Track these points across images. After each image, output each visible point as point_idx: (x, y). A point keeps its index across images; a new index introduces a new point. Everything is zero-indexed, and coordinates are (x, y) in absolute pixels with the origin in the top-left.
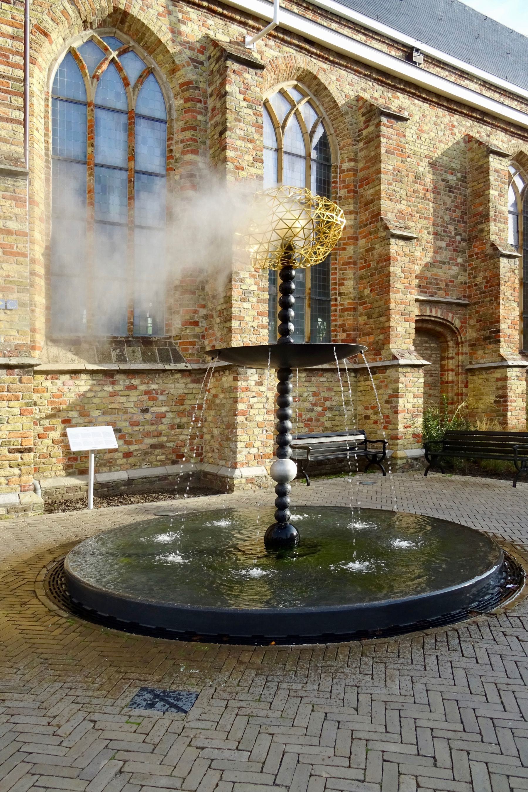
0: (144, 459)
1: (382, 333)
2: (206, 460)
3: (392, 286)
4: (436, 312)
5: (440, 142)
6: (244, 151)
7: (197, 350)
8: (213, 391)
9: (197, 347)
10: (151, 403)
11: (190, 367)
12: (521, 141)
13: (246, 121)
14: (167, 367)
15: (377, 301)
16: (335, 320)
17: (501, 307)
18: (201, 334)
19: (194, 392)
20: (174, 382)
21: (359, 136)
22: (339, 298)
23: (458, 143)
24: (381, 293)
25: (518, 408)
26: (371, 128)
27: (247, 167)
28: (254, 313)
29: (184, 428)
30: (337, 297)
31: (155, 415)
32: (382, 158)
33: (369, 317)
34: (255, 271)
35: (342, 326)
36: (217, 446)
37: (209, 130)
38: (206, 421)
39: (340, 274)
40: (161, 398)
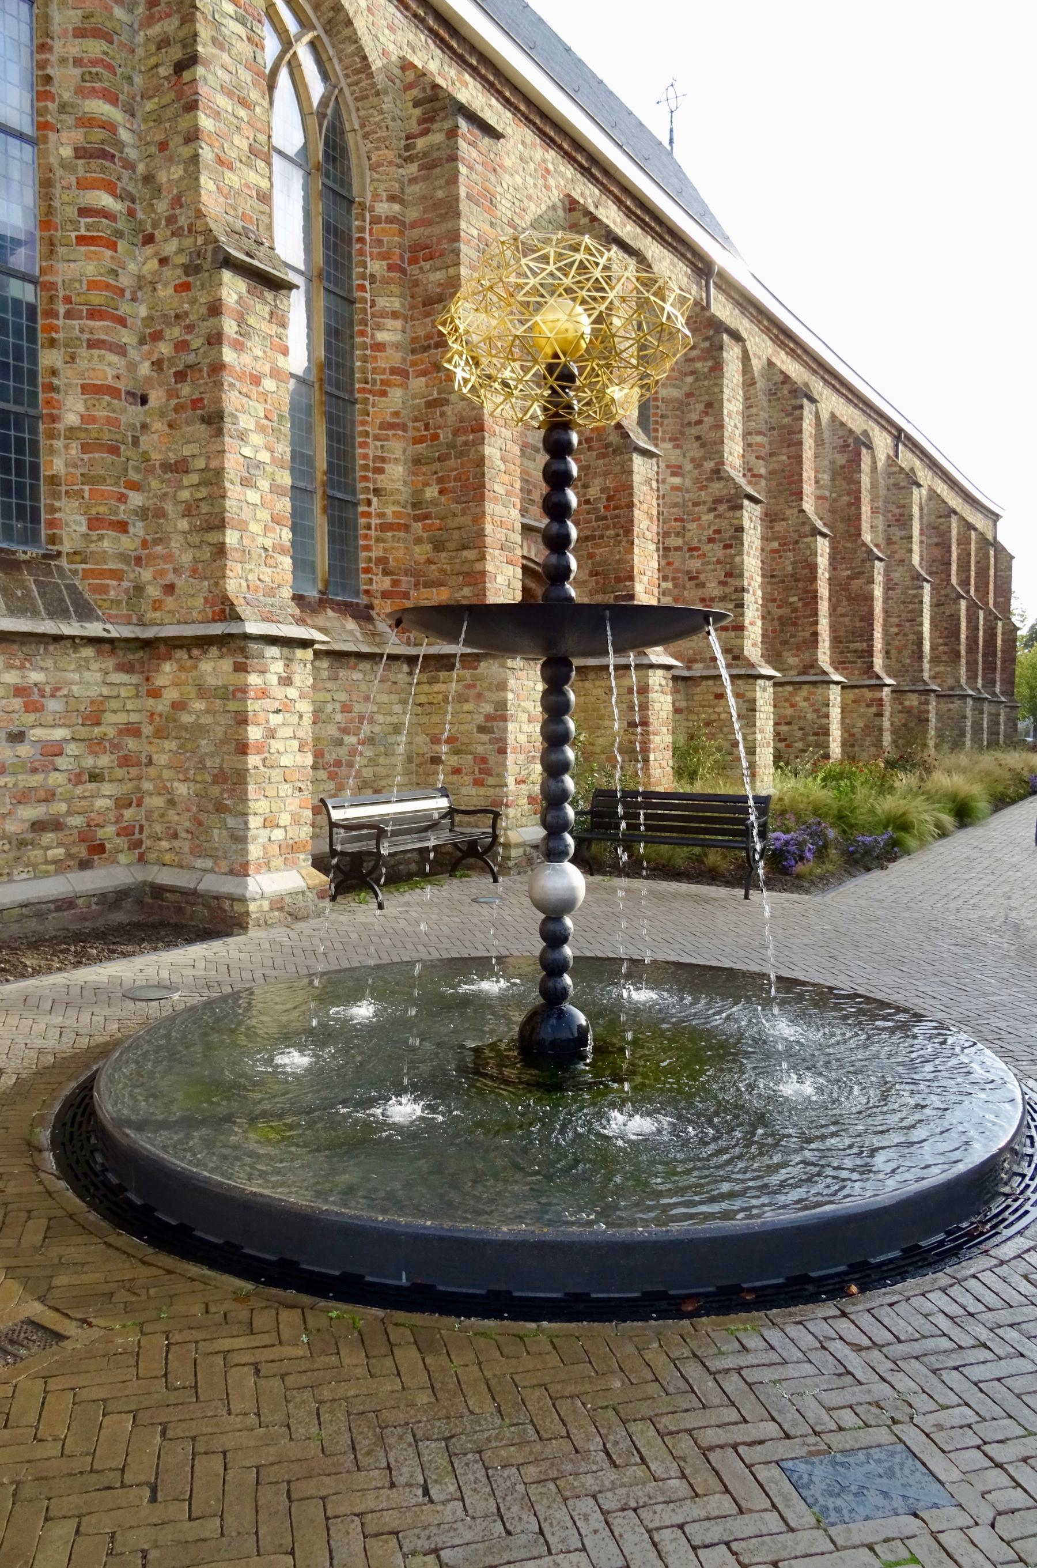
0: (17, 859)
1: (469, 585)
2: (152, 856)
3: (488, 486)
4: (529, 551)
5: (529, 198)
6: (231, 123)
7: (127, 591)
8: (171, 695)
9: (126, 584)
10: (30, 718)
11: (114, 634)
12: (639, 230)
13: (234, 52)
14: (66, 630)
15: (455, 515)
16: (367, 548)
17: (636, 550)
18: (133, 554)
19: (123, 694)
20: (79, 669)
21: (407, 148)
22: (375, 500)
23: (554, 208)
24: (463, 499)
25: (662, 746)
26: (437, 138)
27: (238, 164)
28: (264, 515)
29: (103, 780)
30: (371, 496)
31: (39, 746)
32: (461, 207)
33: (438, 546)
34: (266, 417)
35: (382, 561)
36: (187, 824)
37: (140, 52)
38: (150, 763)
39: (376, 447)
40: (54, 706)
